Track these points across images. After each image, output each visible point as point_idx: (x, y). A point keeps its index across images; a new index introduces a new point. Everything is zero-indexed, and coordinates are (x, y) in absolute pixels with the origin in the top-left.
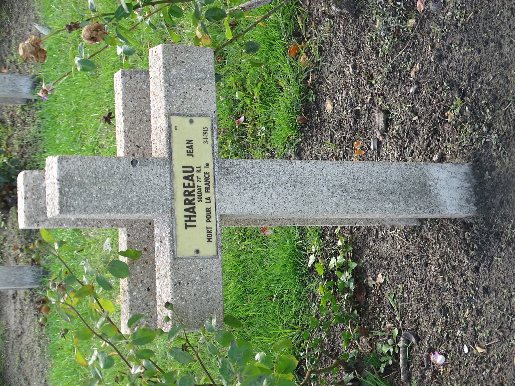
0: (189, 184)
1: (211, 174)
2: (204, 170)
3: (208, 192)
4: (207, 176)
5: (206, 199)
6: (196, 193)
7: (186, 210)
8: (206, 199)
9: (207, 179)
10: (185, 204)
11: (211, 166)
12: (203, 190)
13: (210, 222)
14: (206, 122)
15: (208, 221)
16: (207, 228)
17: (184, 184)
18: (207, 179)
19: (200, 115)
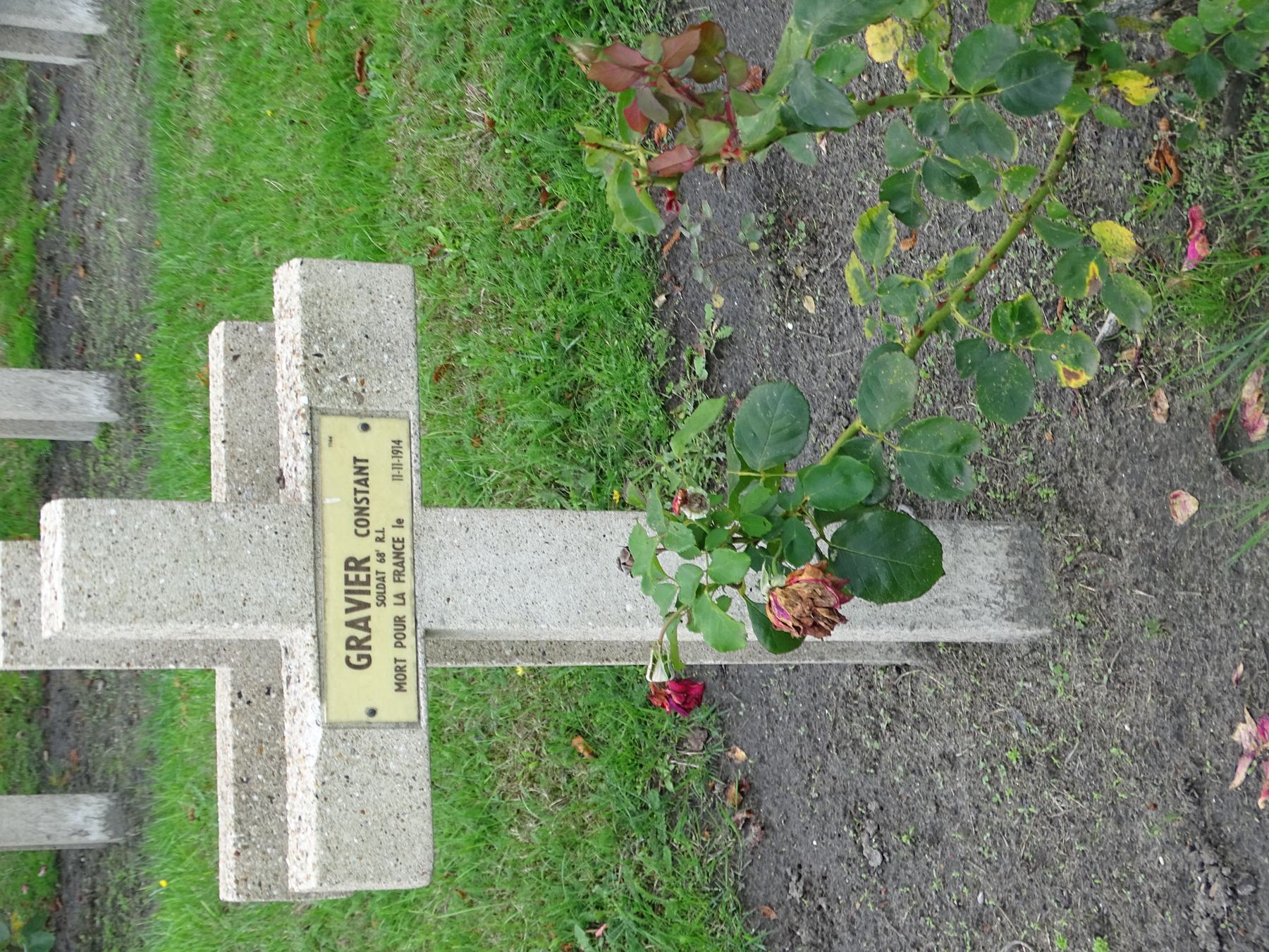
1: (408, 543)
2: (391, 533)
3: (399, 581)
4: (398, 545)
5: (396, 596)
6: (374, 582)
8: (396, 596)
9: (398, 554)
11: (407, 524)
13: (402, 646)
14: (398, 430)
15: (399, 644)
16: (396, 660)
18: (398, 554)
19: (386, 415)
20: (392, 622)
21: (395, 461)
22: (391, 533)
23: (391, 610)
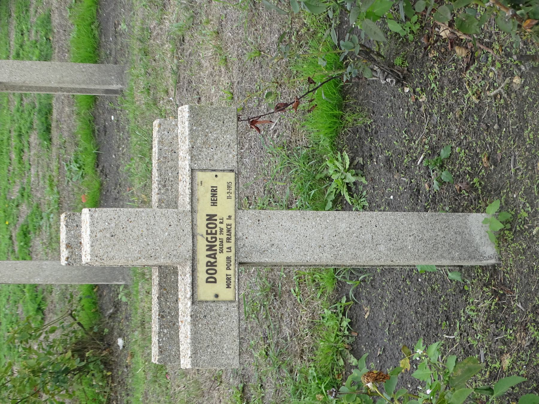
0: (211, 231)
1: (233, 226)
2: (226, 222)
3: (229, 242)
4: (229, 227)
5: (228, 248)
6: (218, 243)
7: (207, 256)
8: (228, 248)
9: (229, 231)
10: (207, 250)
11: (233, 217)
12: (225, 241)
15: (228, 268)
16: (227, 275)
17: (207, 231)
18: (229, 231)
20: (226, 259)
21: (228, 191)
22: (226, 222)
23: (225, 255)
